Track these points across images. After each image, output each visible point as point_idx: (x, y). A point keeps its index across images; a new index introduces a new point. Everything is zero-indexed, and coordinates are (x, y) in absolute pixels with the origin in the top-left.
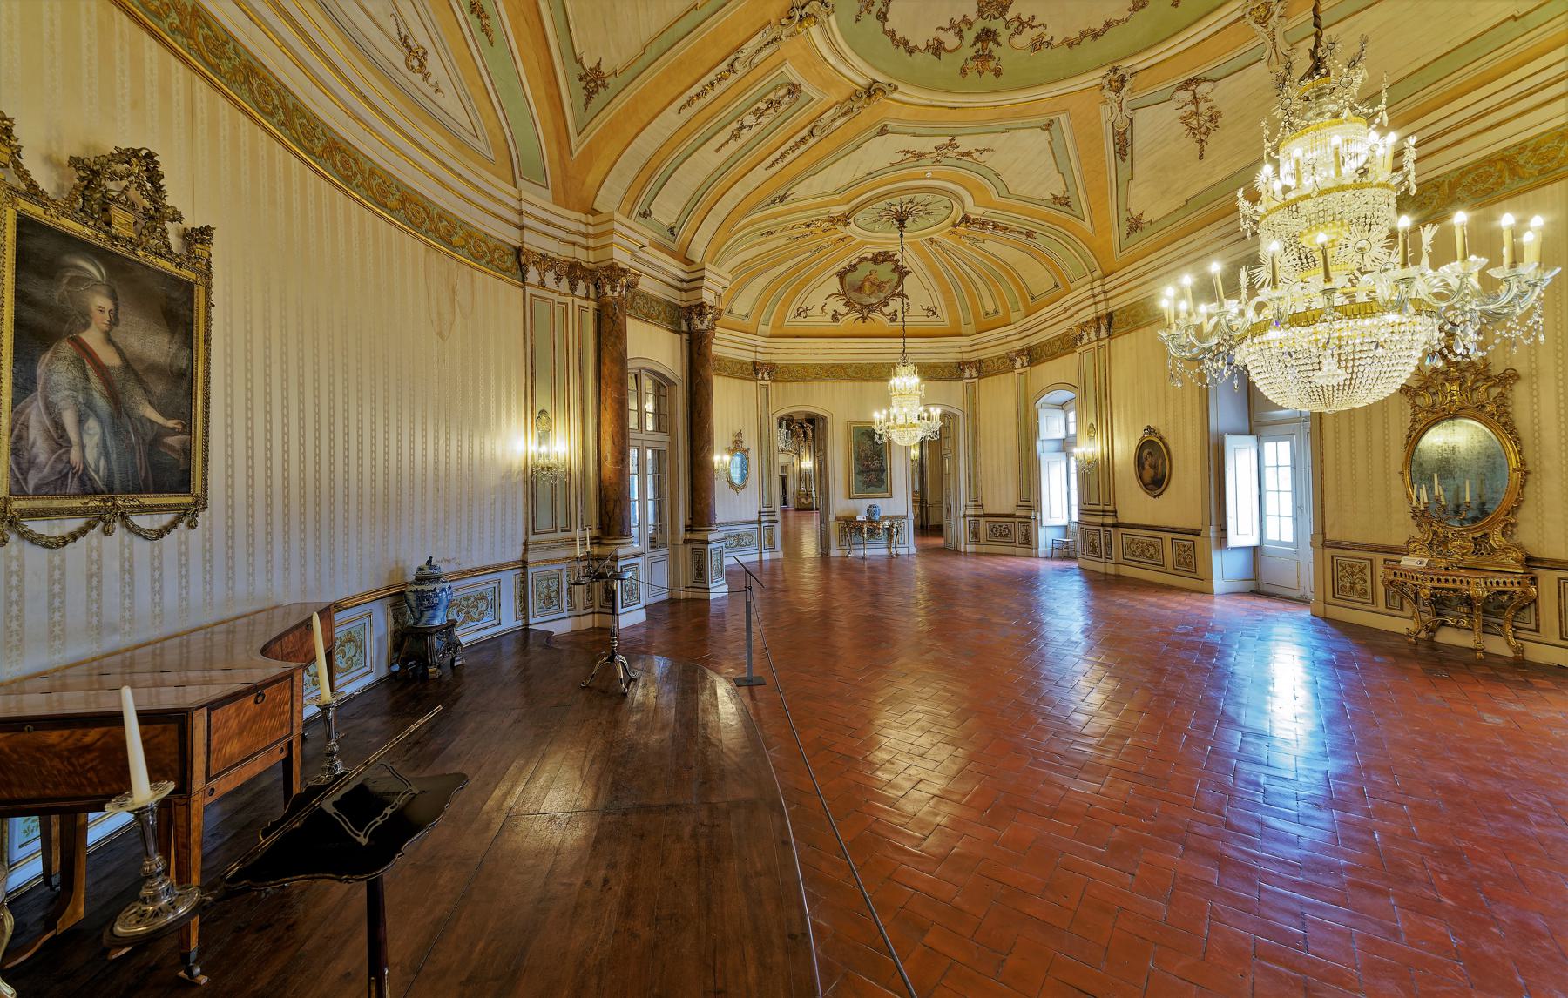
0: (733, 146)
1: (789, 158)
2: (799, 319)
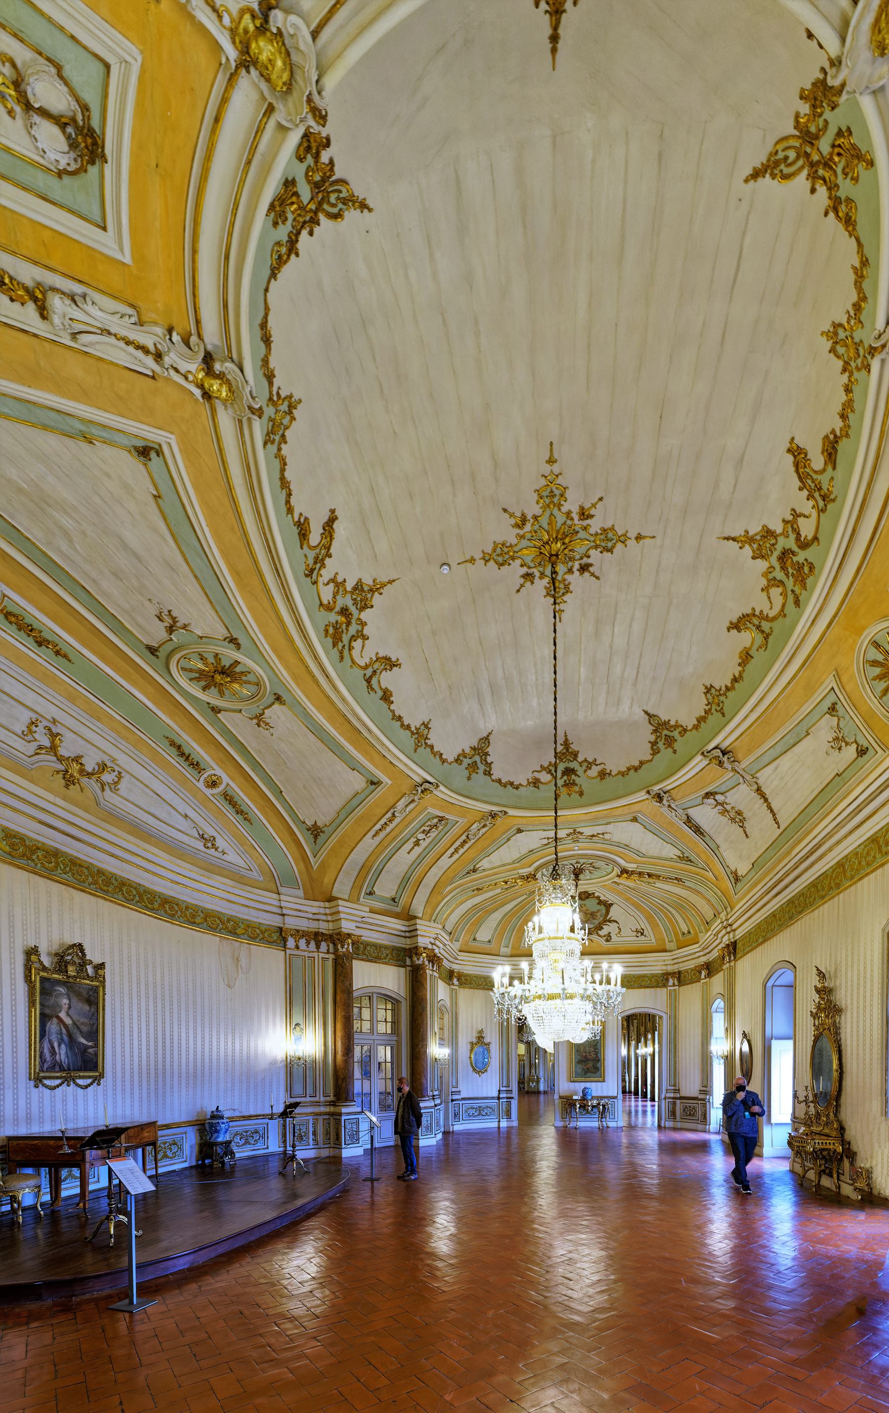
0: (418, 850)
1: (461, 851)
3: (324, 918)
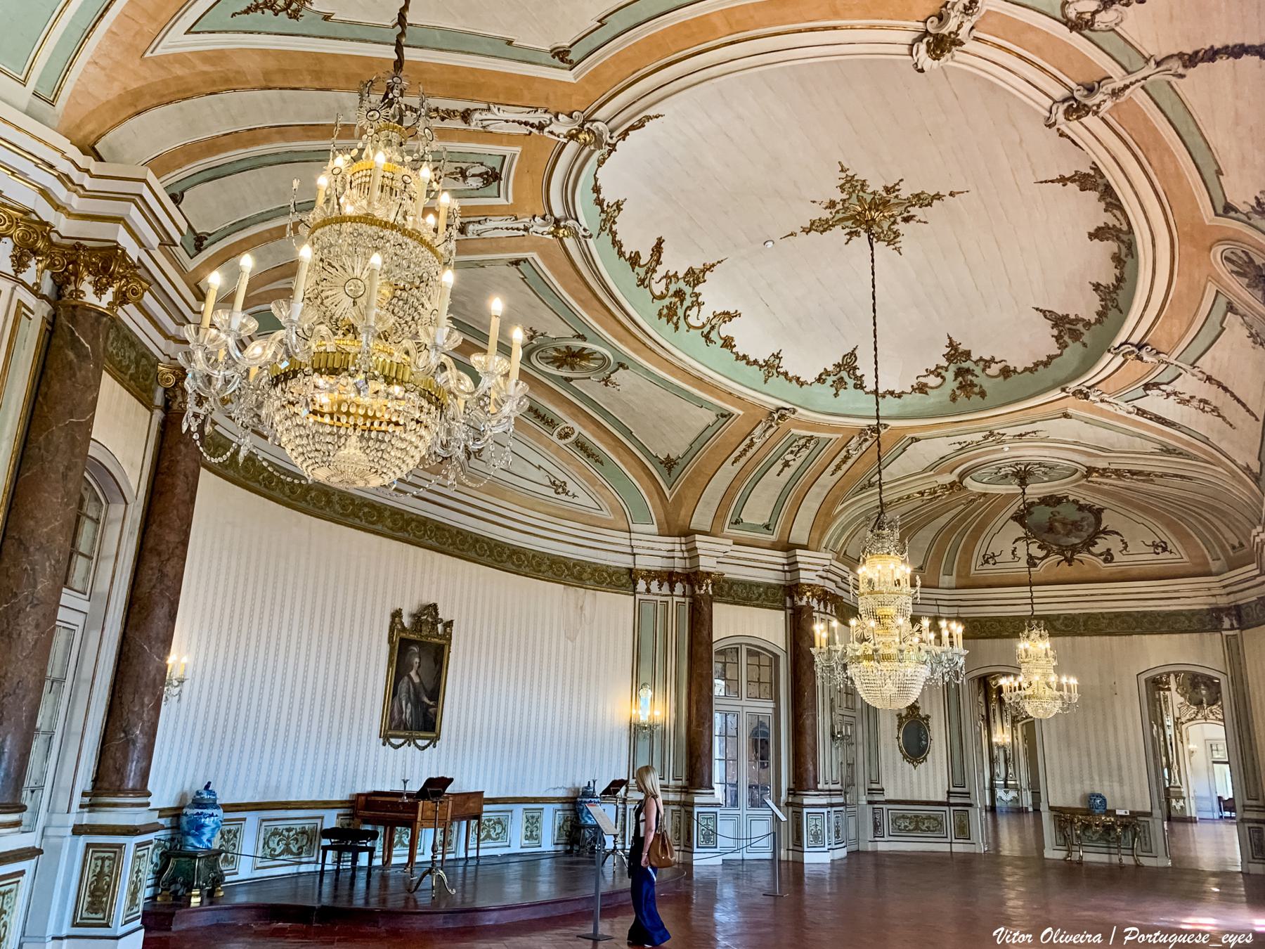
0: (788, 472)
1: (845, 467)
2: (986, 566)
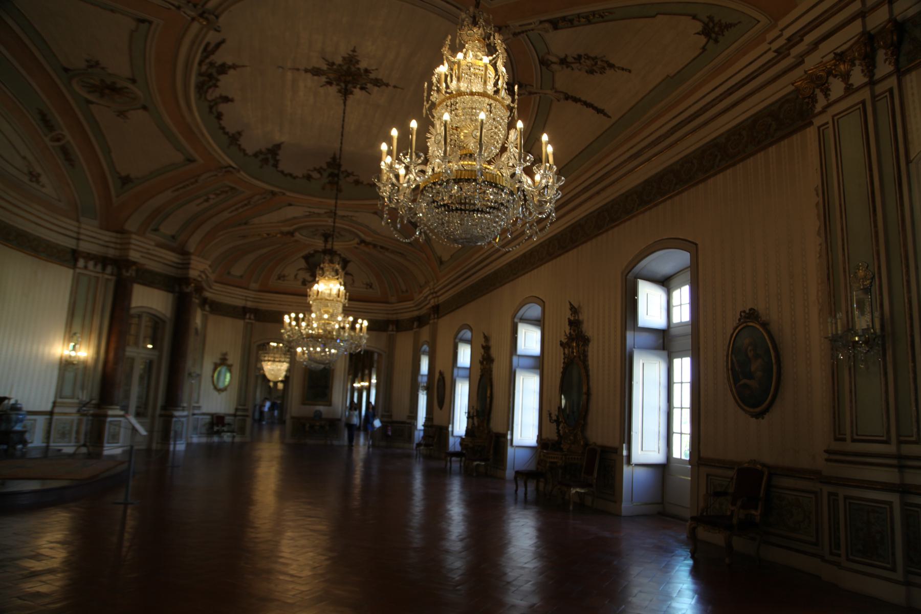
0: (206, 205)
1: (241, 210)
2: (279, 281)
3: (112, 245)
